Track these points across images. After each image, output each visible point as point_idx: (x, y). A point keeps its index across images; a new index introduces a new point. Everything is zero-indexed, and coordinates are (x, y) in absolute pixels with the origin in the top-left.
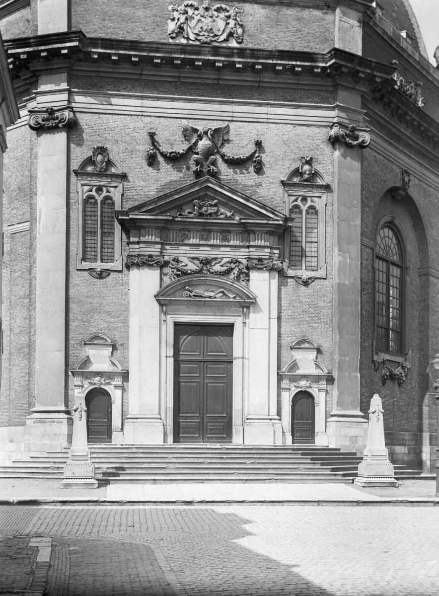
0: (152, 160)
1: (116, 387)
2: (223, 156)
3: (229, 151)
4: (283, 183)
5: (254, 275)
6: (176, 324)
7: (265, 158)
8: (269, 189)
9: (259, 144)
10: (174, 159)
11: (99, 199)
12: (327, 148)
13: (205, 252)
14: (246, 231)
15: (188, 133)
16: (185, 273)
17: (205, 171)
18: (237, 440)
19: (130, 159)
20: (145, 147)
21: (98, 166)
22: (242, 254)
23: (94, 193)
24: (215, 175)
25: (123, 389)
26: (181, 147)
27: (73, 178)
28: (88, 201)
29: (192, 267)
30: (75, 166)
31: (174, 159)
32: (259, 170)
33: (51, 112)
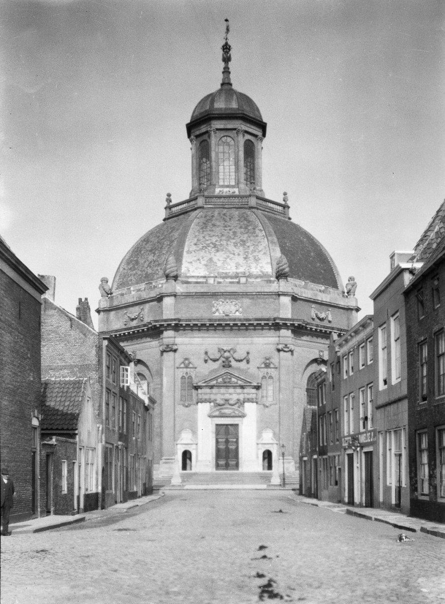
0: (206, 361)
1: (194, 449)
2: (234, 358)
3: (236, 356)
4: (258, 368)
5: (246, 404)
6: (217, 425)
7: (251, 357)
8: (253, 370)
9: (248, 353)
10: (215, 360)
11: (187, 377)
12: (276, 353)
13: (227, 396)
14: (242, 387)
15: (220, 350)
16: (219, 405)
17: (227, 365)
18: (240, 469)
19: (197, 361)
20: (203, 356)
21: (187, 363)
22: (241, 397)
23: (184, 375)
24: (230, 366)
25: (197, 449)
26: (217, 356)
27: (176, 369)
28: (183, 378)
29: (222, 402)
30: (177, 365)
31: (215, 360)
32: (248, 362)
33: (168, 346)
